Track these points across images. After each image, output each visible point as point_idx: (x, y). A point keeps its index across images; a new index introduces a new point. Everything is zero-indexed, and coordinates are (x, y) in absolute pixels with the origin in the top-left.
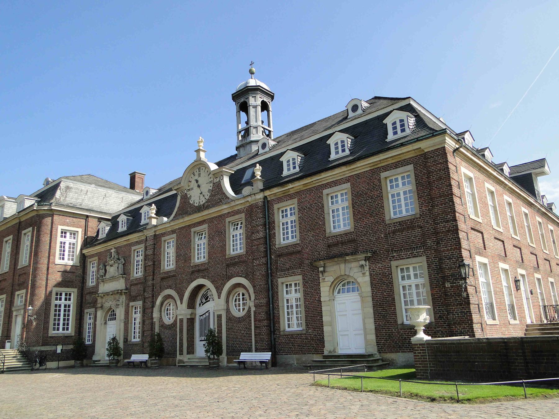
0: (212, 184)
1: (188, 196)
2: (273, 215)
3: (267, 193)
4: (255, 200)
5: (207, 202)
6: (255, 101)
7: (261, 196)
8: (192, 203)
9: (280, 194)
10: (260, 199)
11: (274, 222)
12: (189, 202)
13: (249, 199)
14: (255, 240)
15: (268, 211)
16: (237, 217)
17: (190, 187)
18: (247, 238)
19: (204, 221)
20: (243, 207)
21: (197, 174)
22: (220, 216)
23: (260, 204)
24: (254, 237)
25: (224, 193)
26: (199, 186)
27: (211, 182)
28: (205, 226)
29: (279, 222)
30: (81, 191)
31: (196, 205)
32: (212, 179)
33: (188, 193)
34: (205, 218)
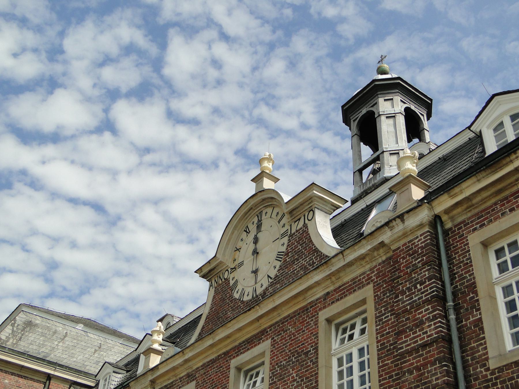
0: (286, 240)
1: (232, 282)
2: (469, 265)
3: (444, 203)
4: (405, 235)
5: (271, 285)
6: (391, 110)
7: (424, 215)
8: (236, 296)
9: (484, 201)
10: (421, 226)
11: (473, 287)
12: (231, 296)
13: (386, 236)
14: (409, 353)
15: (450, 260)
16: (351, 299)
17: (236, 263)
18: (384, 351)
19: (263, 332)
20: (368, 267)
21: (253, 228)
22: (305, 309)
23: (421, 240)
24: (407, 343)
25: (317, 251)
26: (255, 252)
27: (283, 235)
28: (265, 345)
29: (492, 285)
30: (55, 332)
32: (287, 227)
33: (231, 276)
34: (265, 323)
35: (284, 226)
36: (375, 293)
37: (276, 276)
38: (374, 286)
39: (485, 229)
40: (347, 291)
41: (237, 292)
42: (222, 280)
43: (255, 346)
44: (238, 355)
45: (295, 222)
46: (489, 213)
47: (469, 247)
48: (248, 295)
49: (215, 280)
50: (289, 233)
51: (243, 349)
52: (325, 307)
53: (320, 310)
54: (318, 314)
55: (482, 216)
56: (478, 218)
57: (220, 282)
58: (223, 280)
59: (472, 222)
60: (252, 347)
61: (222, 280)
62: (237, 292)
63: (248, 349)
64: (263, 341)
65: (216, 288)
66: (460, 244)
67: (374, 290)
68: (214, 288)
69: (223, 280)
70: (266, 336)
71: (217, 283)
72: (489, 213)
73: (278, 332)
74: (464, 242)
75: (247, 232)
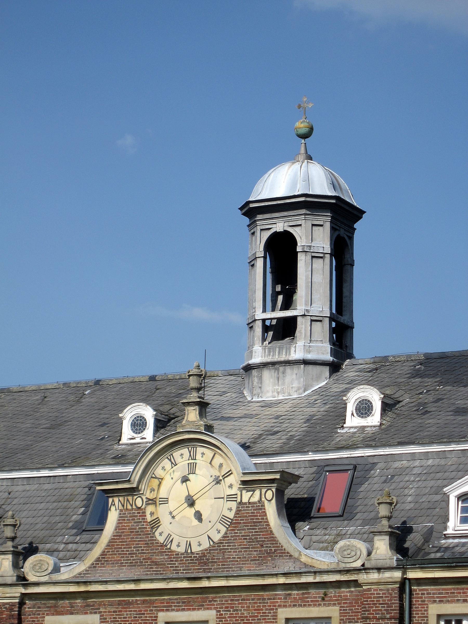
0: (234, 505)
1: (149, 518)
7: (398, 575)
8: (161, 539)
10: (395, 583)
27: (231, 498)
31: (174, 547)
33: (150, 509)
35: (231, 486)
36: (341, 616)
37: (220, 542)
38: (340, 610)
39: (442, 605)
40: (312, 601)
41: (161, 534)
42: (132, 506)
43: (194, 609)
44: (167, 610)
45: (248, 491)
46: (448, 593)
47: (427, 614)
48: (178, 546)
49: (119, 500)
50: (239, 500)
51: (175, 606)
52: (285, 606)
53: (280, 606)
54: (277, 609)
55: (442, 593)
56: (439, 593)
57: (129, 507)
58: (134, 507)
59: (434, 594)
60: (189, 610)
61: (132, 506)
62: (161, 534)
63: (183, 610)
65: (121, 510)
66: (421, 608)
67: (340, 613)
68: (118, 511)
69: (134, 507)
70: (208, 605)
71: (123, 506)
72: (448, 593)
73: (226, 607)
74: (424, 607)
75: (172, 463)
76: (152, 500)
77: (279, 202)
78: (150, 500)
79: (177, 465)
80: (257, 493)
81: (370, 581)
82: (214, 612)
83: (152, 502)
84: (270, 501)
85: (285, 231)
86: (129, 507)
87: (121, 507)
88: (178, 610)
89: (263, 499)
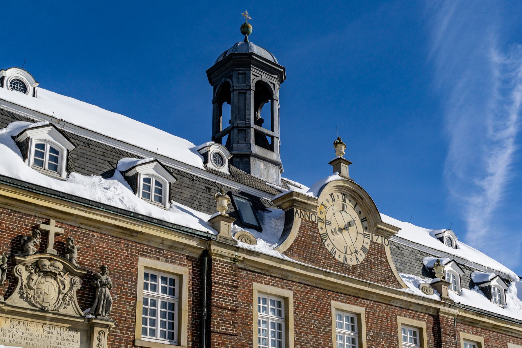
0: (368, 241)
42: (309, 218)
57: (308, 219)
64: (358, 305)
76: (322, 219)
77: (273, 66)
78: (320, 219)
79: (335, 201)
80: (380, 238)
81: (445, 311)
82: (363, 309)
83: (321, 220)
84: (387, 246)
85: (267, 83)
86: (308, 219)
87: (302, 217)
88: (342, 302)
89: (384, 244)
